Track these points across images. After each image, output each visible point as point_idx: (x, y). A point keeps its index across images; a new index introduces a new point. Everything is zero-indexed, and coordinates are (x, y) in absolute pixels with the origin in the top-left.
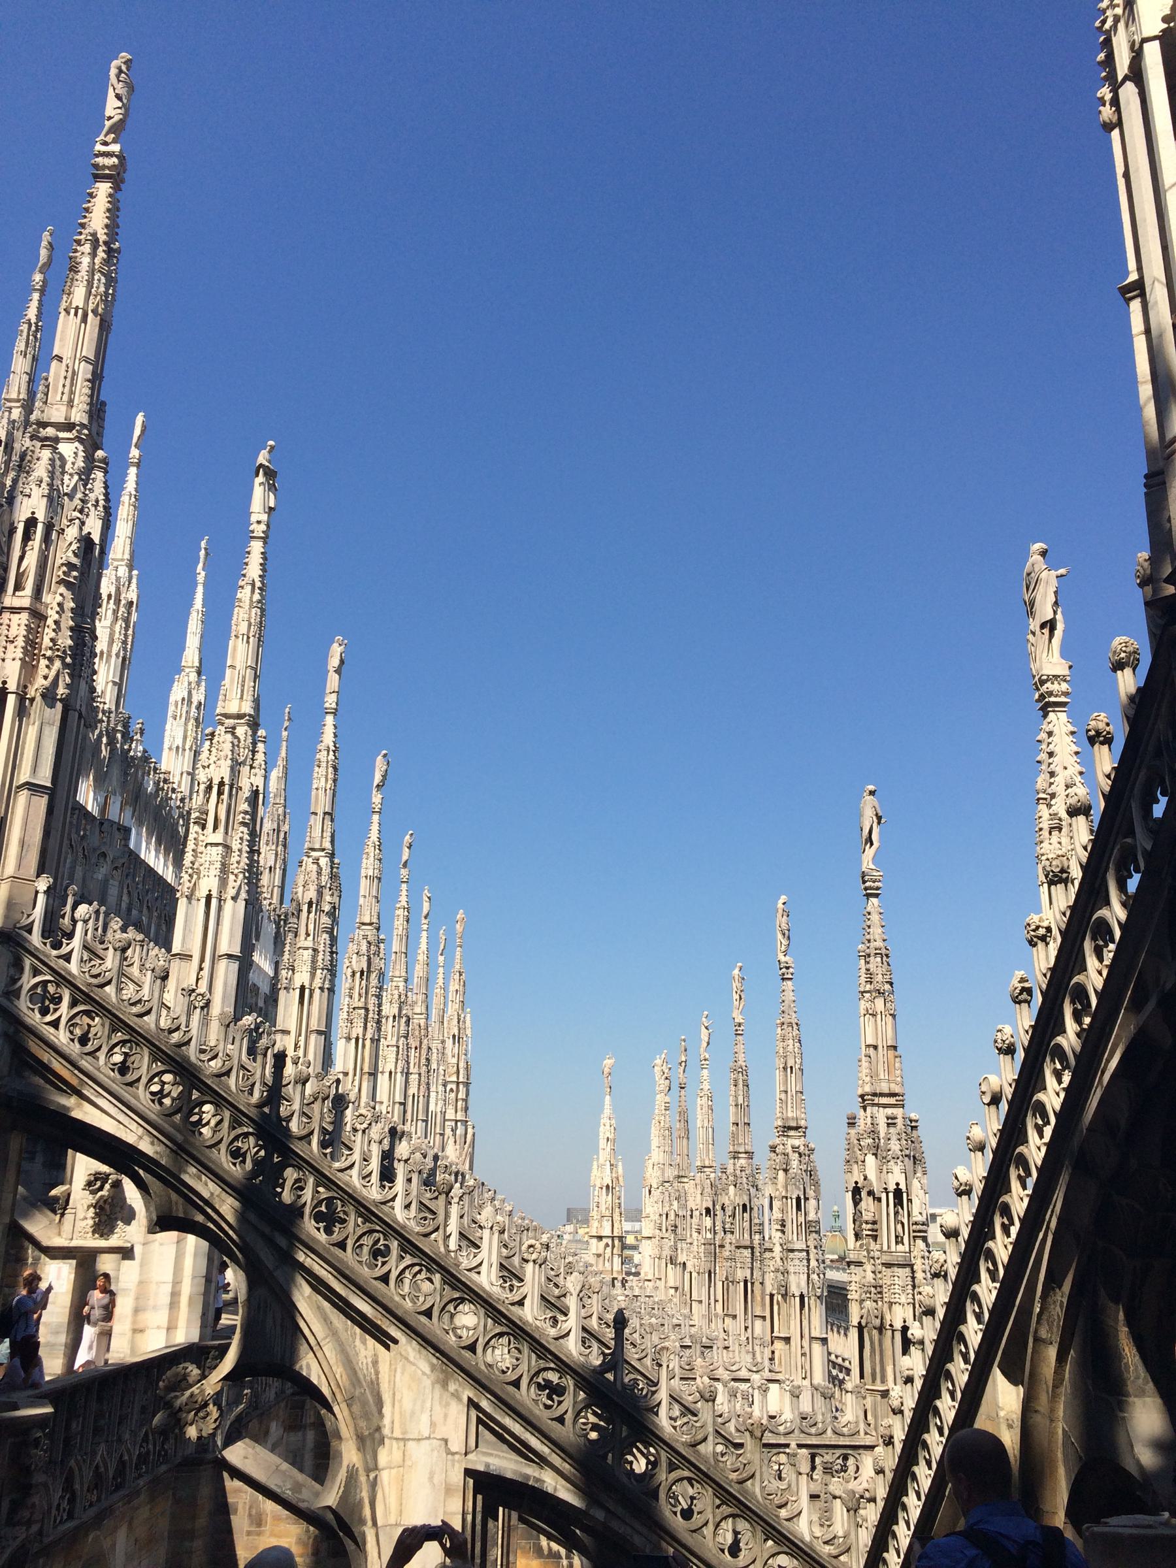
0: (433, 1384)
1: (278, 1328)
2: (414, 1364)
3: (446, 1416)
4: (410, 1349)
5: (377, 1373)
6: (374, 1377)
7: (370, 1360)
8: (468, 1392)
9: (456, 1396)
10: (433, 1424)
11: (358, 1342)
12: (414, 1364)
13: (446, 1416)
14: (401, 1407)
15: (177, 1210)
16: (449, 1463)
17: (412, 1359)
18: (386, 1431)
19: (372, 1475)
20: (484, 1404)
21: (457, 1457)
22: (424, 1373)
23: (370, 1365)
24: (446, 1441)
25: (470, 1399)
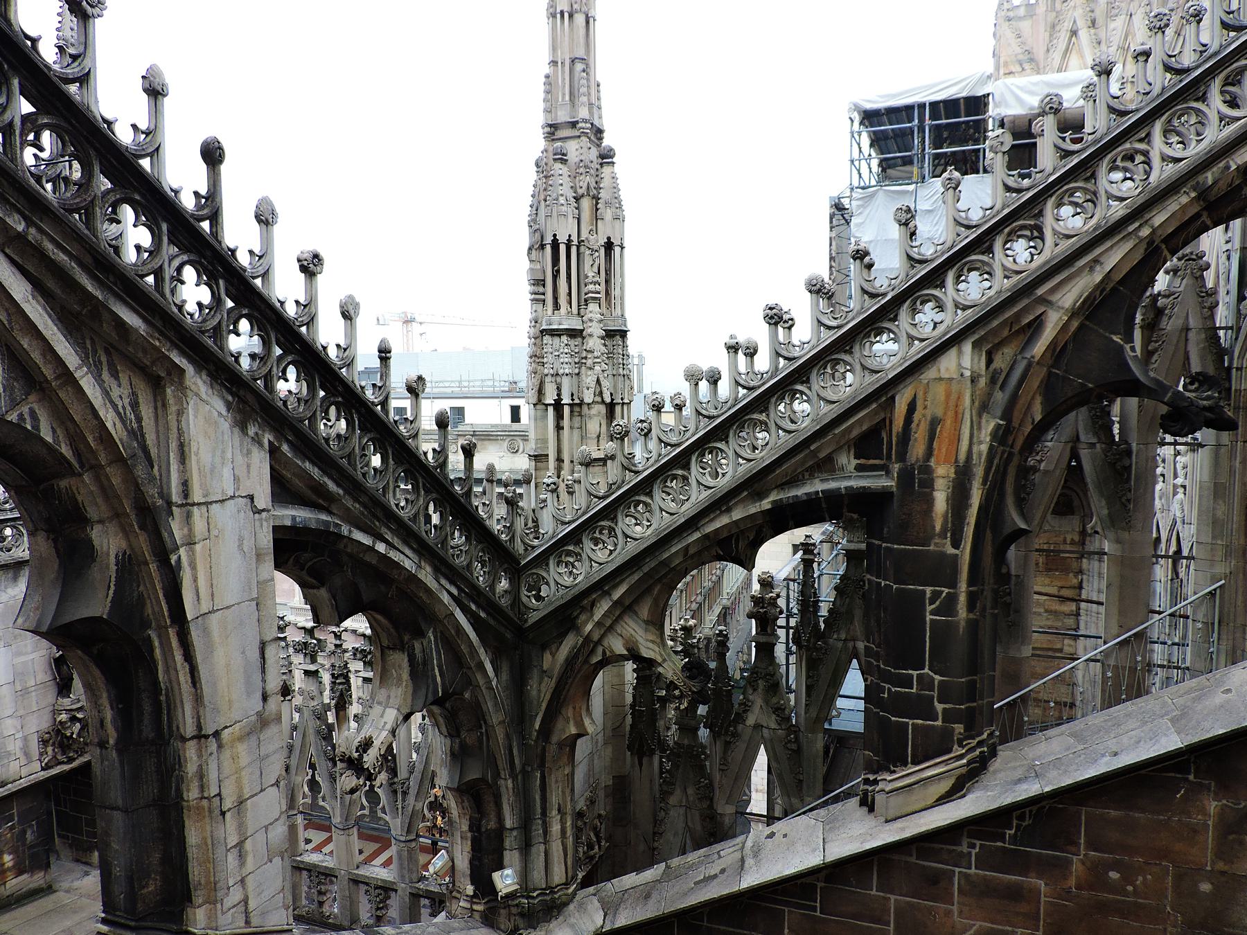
0: (232, 427)
3: (248, 466)
4: (200, 382)
5: (139, 419)
6: (135, 426)
7: (127, 401)
9: (257, 440)
10: (236, 479)
13: (248, 466)
14: (198, 462)
16: (257, 523)
17: (204, 396)
18: (176, 498)
19: (173, 559)
21: (264, 514)
22: (220, 414)
23: (128, 408)
24: (251, 498)
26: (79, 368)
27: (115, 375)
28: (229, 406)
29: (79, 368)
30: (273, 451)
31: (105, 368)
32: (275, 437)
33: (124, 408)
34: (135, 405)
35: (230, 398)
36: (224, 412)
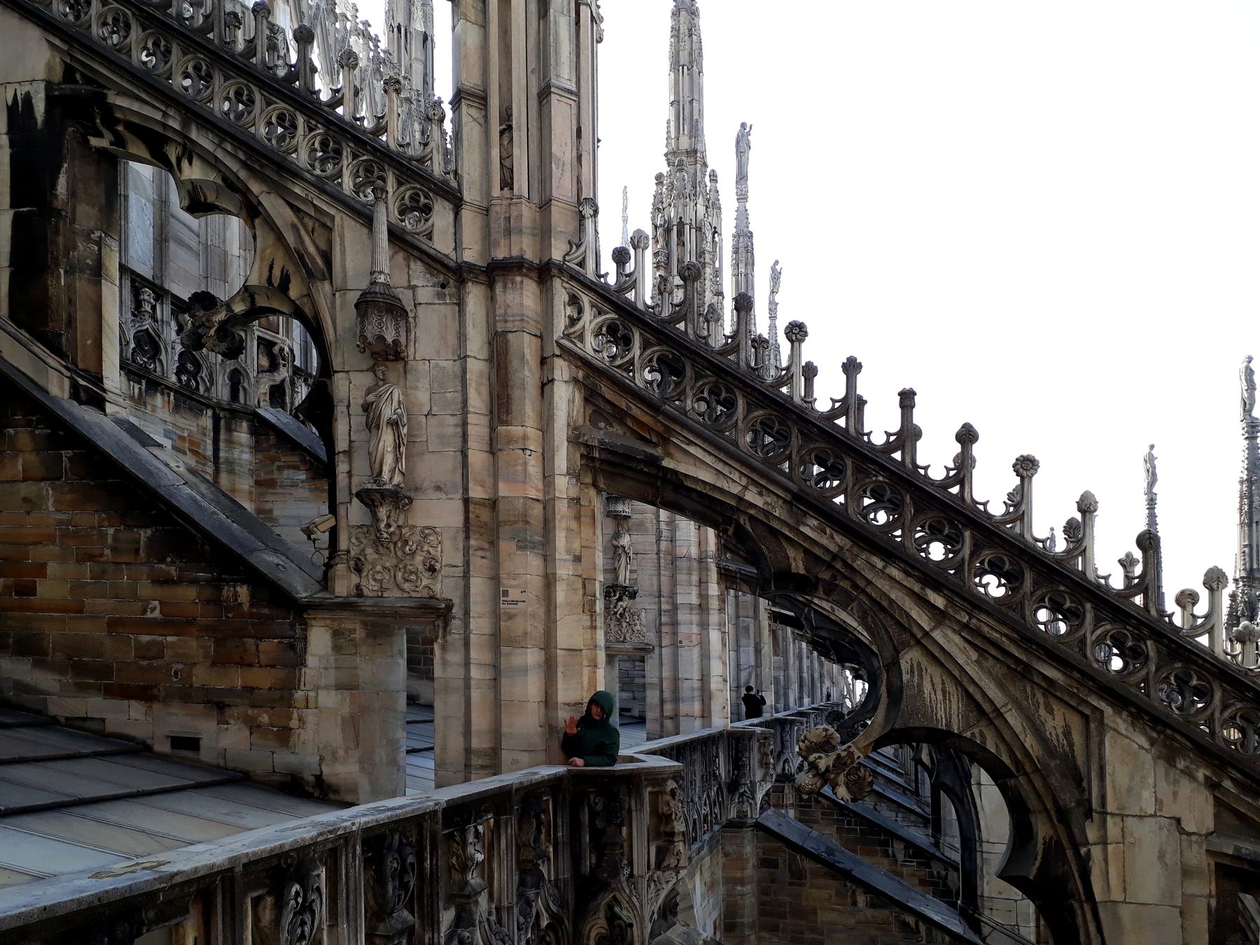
1: (939, 693)
2: (1126, 737)
4: (1119, 720)
5: (1071, 745)
6: (1067, 749)
7: (1060, 731)
8: (1201, 774)
11: (1042, 711)
12: (1126, 737)
15: (797, 566)
17: (1123, 732)
20: (1227, 784)
22: (1141, 747)
23: (1061, 736)
25: (1206, 777)
26: (1005, 705)
27: (1050, 711)
28: (1153, 742)
29: (1005, 705)
30: (1212, 785)
31: (1042, 707)
32: (1214, 773)
33: (1057, 736)
34: (1067, 734)
35: (1155, 735)
36: (1147, 746)
